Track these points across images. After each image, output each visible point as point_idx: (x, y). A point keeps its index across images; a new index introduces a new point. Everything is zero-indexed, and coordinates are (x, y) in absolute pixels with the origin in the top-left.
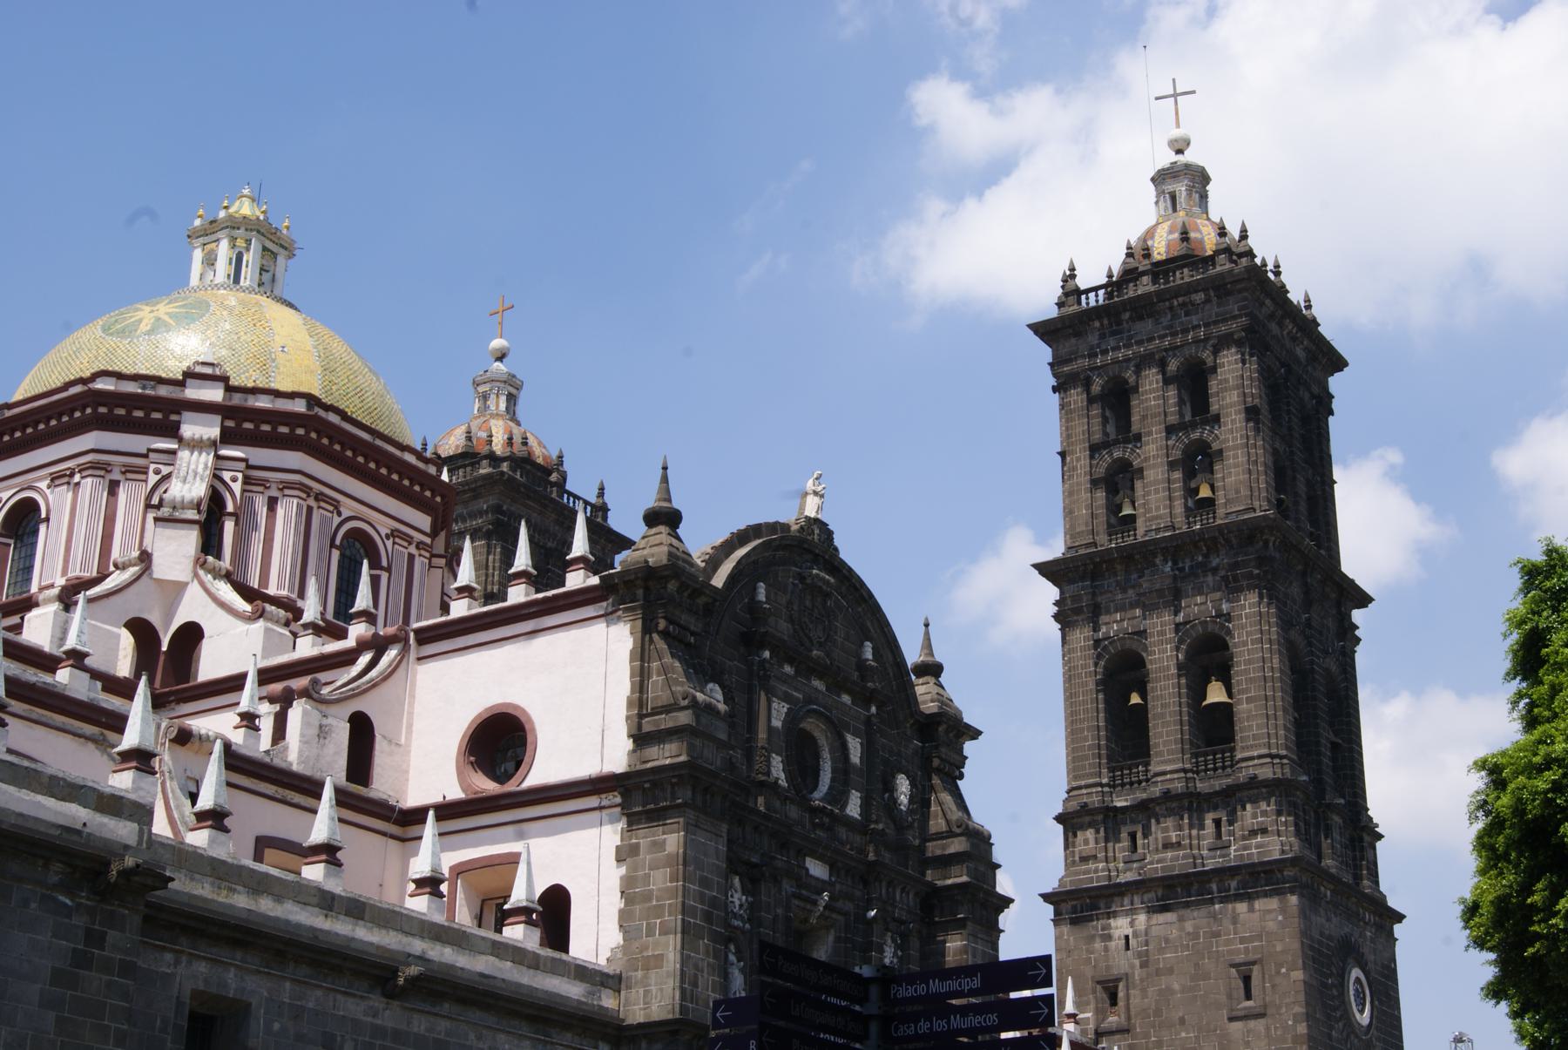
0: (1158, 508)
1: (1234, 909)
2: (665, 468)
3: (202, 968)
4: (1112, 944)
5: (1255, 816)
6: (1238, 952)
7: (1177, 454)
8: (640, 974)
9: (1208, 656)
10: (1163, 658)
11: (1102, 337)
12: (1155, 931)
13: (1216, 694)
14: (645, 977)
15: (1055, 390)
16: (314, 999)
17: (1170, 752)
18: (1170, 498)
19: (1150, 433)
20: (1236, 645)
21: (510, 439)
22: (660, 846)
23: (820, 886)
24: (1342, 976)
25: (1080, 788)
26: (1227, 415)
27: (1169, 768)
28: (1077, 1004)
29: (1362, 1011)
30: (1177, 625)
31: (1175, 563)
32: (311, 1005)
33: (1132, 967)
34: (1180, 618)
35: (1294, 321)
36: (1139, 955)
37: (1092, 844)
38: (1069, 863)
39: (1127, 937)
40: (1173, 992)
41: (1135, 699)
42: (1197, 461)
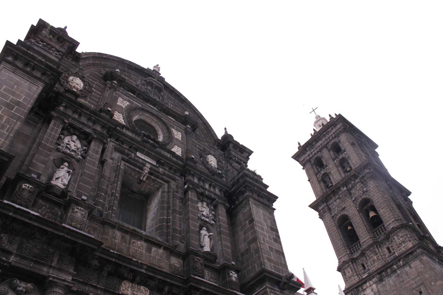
0: (337, 178)
1: (405, 271)
5: (399, 239)
6: (413, 284)
10: (353, 212)
15: (303, 169)
18: (340, 174)
19: (329, 163)
20: (372, 197)
27: (366, 239)
30: (353, 201)
31: (347, 187)
34: (353, 199)
37: (351, 272)
38: (346, 280)
41: (349, 228)
42: (343, 164)
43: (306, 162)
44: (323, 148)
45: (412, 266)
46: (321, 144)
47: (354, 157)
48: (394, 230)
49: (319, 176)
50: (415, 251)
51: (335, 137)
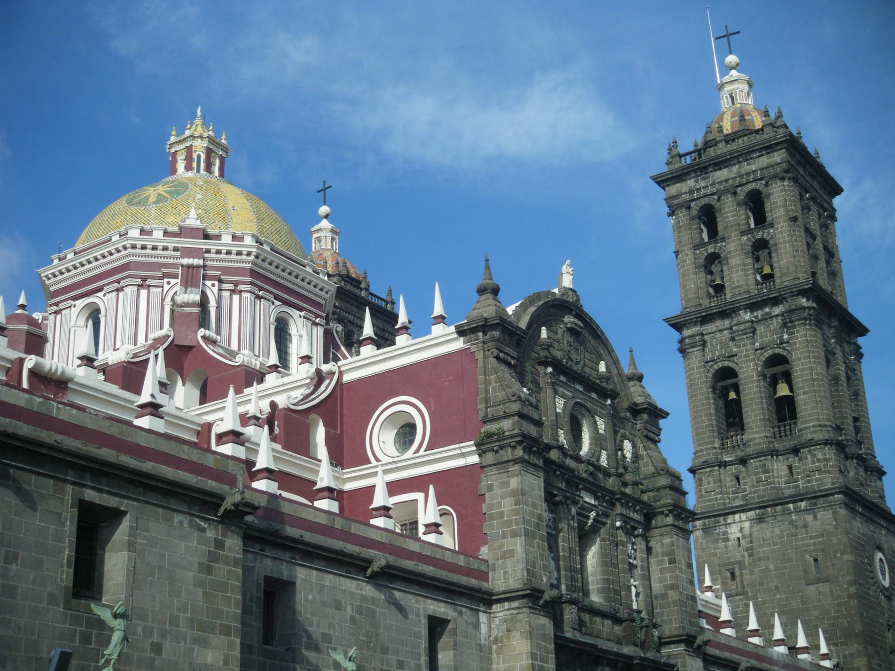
0: (738, 281)
1: (805, 519)
2: (487, 260)
3: (268, 562)
4: (730, 543)
5: (813, 462)
6: (809, 545)
7: (748, 248)
8: (500, 562)
9: (777, 367)
10: (749, 372)
11: (697, 181)
12: (755, 535)
13: (783, 390)
14: (504, 563)
16: (329, 579)
17: (757, 427)
19: (730, 237)
21: (337, 263)
22: (507, 484)
23: (592, 508)
24: (871, 558)
25: (702, 451)
26: (778, 223)
27: (757, 436)
28: (713, 580)
29: (884, 579)
32: (327, 584)
33: (743, 556)
35: (812, 166)
36: (747, 549)
39: (739, 539)
40: (770, 571)
41: (732, 395)
43: (680, 206)
44: (726, 191)
45: (819, 517)
46: (727, 180)
47: (786, 253)
48: (812, 443)
49: (701, 253)
50: (832, 494)
51: (762, 179)
